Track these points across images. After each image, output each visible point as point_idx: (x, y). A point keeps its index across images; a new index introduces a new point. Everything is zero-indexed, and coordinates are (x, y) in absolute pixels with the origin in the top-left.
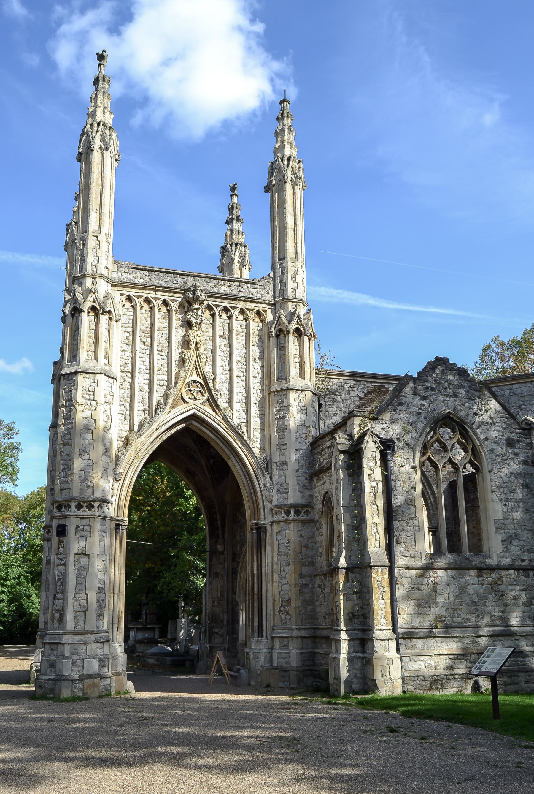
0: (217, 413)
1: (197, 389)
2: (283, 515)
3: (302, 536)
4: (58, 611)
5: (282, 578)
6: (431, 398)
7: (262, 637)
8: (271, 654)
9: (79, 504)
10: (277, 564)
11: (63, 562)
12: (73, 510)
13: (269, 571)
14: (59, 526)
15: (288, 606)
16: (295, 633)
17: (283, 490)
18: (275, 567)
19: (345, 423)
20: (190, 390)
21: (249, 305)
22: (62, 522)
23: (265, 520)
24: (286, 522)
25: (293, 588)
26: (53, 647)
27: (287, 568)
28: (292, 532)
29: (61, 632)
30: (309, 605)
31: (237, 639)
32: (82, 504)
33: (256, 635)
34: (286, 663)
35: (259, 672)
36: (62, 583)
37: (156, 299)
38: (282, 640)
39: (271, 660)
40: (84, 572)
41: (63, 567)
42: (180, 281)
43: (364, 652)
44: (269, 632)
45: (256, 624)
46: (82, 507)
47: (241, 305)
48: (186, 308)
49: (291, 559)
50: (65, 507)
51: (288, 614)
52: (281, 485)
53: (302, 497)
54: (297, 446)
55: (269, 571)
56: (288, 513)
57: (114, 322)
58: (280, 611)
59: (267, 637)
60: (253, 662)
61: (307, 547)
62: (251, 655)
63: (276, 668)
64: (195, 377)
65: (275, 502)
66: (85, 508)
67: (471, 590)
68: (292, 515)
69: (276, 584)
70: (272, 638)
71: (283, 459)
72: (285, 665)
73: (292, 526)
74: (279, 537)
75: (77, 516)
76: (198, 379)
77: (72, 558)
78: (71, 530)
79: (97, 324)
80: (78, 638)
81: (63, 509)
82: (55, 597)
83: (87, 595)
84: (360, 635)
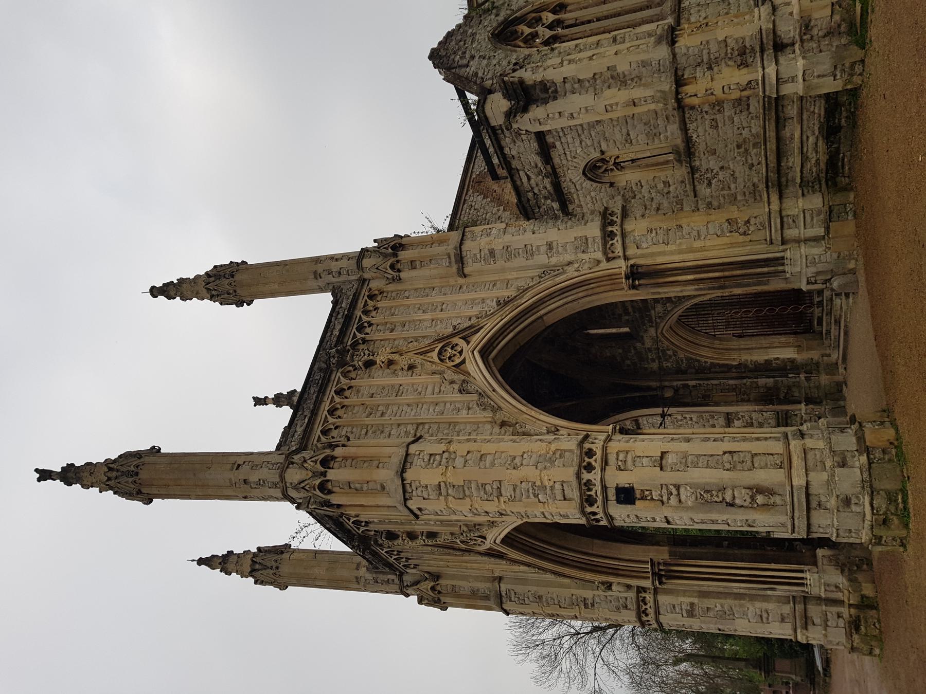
0: (482, 328)
1: (450, 350)
2: (614, 241)
3: (643, 216)
4: (753, 498)
5: (699, 236)
6: (473, 52)
7: (783, 258)
8: (806, 240)
9: (585, 468)
10: (680, 243)
11: (674, 492)
12: (594, 476)
13: (691, 256)
14: (619, 501)
15: (737, 223)
16: (775, 206)
17: (583, 244)
18: (684, 247)
19: (493, 128)
20: (450, 358)
21: (360, 304)
22: (612, 494)
23: (621, 266)
24: (624, 236)
25: (713, 217)
26: (814, 504)
27: (686, 229)
28: (637, 227)
29: (788, 488)
30: (735, 199)
31: (792, 361)
32: (585, 464)
33: (780, 268)
34: (818, 215)
35: (835, 255)
36: (707, 491)
37: (332, 400)
38: (786, 226)
39: (816, 239)
40: (690, 459)
41: (682, 490)
43: (793, 44)
44: (776, 249)
45: (766, 270)
46: (589, 464)
47: (358, 313)
48: (351, 368)
49: (672, 224)
50: (590, 490)
51: (748, 221)
52: (577, 248)
53: (592, 220)
54: (528, 234)
55: (691, 256)
56: (612, 235)
57: (348, 443)
58: (745, 234)
59: (783, 251)
60: (820, 267)
61: (658, 209)
62: (811, 271)
63: (828, 229)
64: (435, 354)
65: (599, 255)
66: (592, 461)
68: (615, 229)
69: (708, 243)
70: (783, 242)
71: (543, 249)
72: (822, 217)
73: (628, 227)
74: (644, 245)
75: (603, 470)
76: (437, 350)
77: (669, 477)
78: (624, 479)
79: (345, 458)
80: (797, 461)
81: (592, 493)
82: (732, 505)
83: (725, 453)
84: (770, 51)
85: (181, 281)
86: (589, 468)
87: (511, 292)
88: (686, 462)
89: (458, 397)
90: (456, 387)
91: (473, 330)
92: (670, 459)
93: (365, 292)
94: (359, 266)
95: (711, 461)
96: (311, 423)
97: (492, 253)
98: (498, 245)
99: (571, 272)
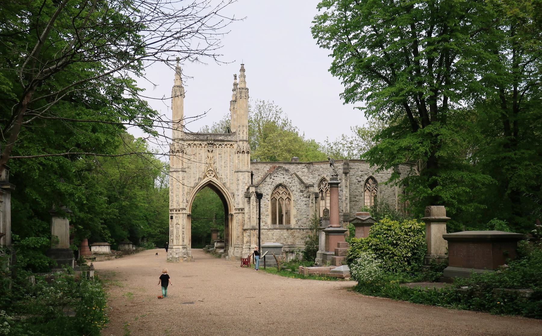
12: (174, 212)
21: (228, 143)
42: (205, 137)
47: (225, 143)
64: (211, 168)
67: (284, 235)
77: (174, 226)
78: (174, 217)
85: (245, 77)
86: (176, 211)
87: (228, 185)
88: (177, 229)
89: (198, 177)
90: (201, 177)
91: (217, 178)
92: (178, 226)
93: (232, 143)
94: (240, 141)
95: (177, 233)
96: (191, 140)
97: (238, 180)
98: (240, 182)
99: (233, 200)
